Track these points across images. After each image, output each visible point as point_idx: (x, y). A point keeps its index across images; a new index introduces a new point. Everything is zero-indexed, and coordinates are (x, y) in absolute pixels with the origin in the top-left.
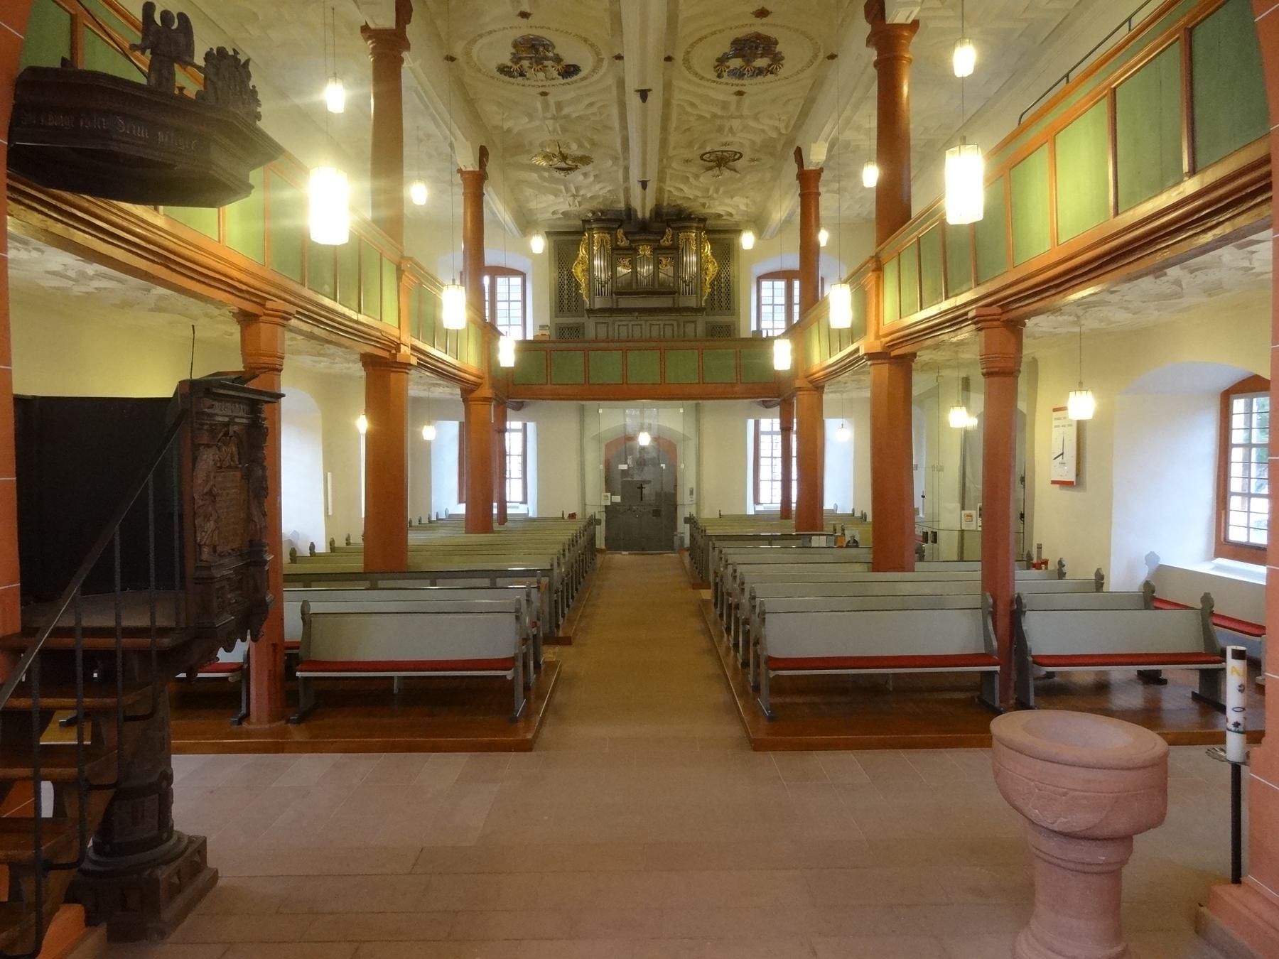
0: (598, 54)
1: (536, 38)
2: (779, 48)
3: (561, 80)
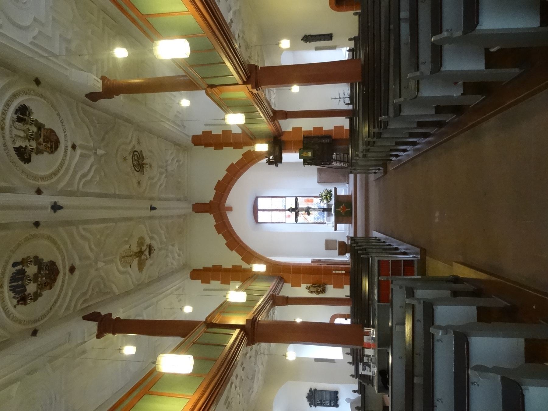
0: (43, 178)
1: (57, 148)
2: (46, 293)
3: (11, 146)
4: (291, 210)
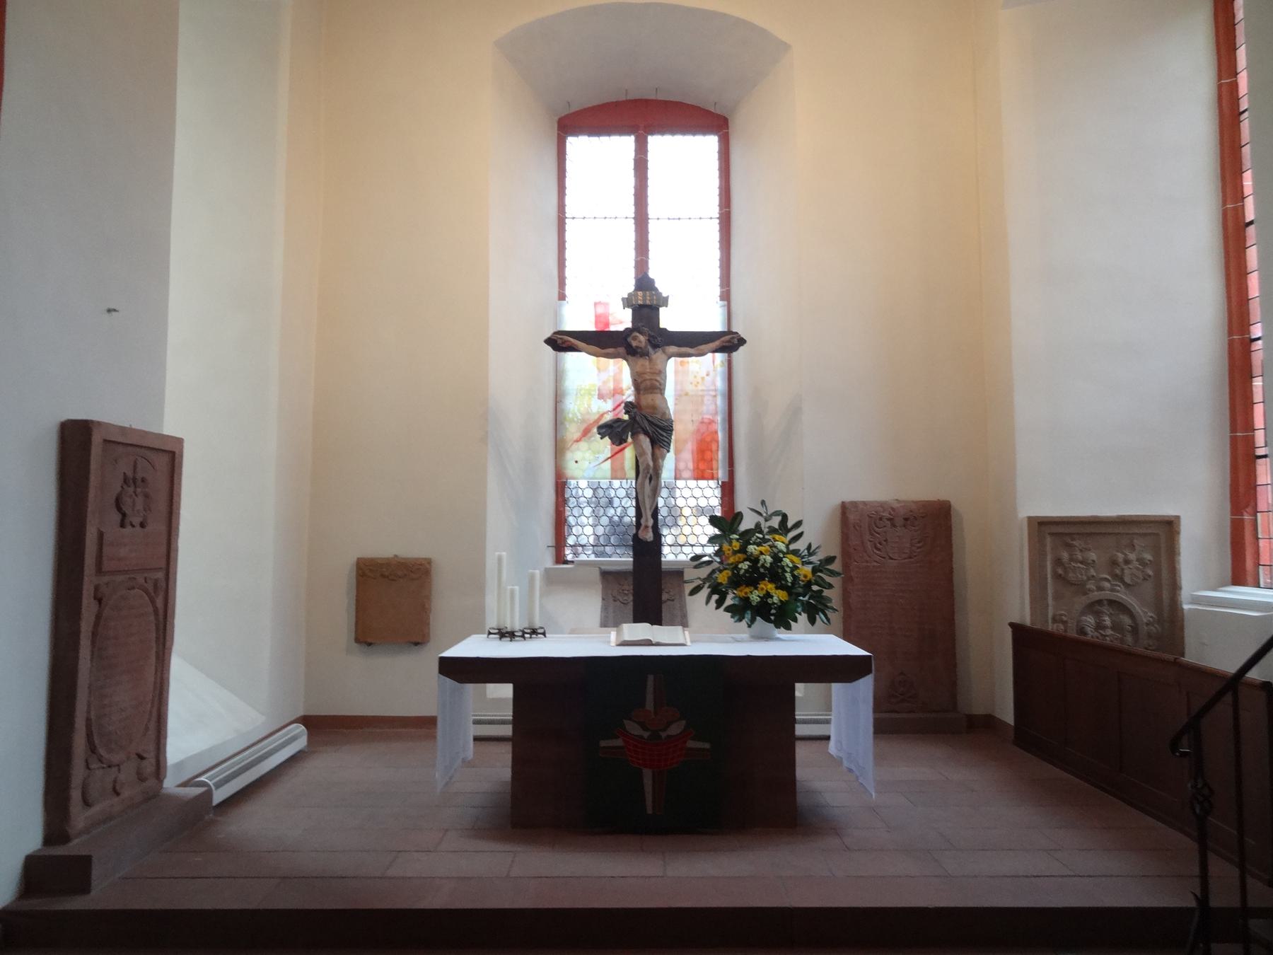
4: (646, 304)
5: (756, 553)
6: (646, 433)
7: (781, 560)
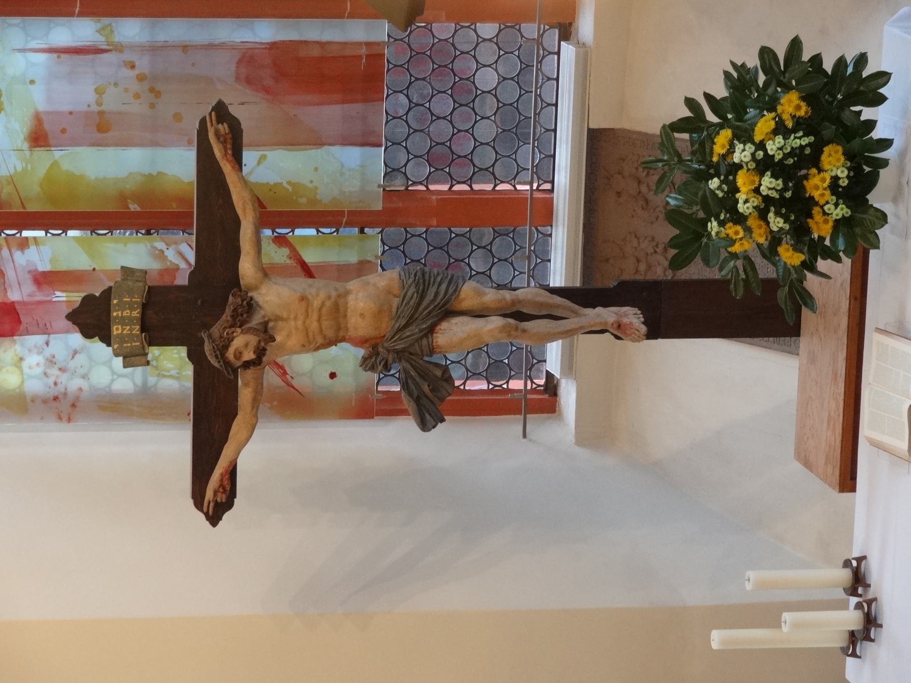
5: (755, 201)
6: (431, 330)
7: (768, 158)
